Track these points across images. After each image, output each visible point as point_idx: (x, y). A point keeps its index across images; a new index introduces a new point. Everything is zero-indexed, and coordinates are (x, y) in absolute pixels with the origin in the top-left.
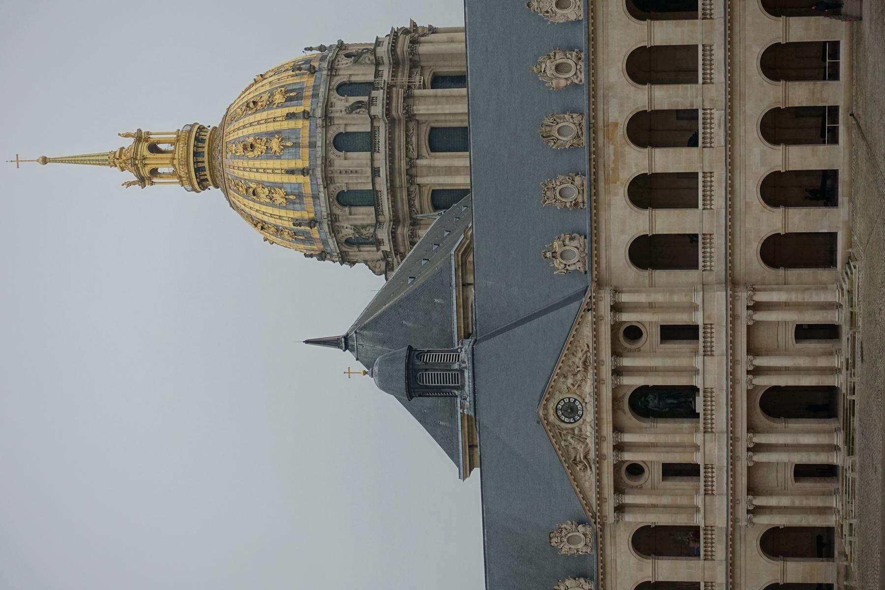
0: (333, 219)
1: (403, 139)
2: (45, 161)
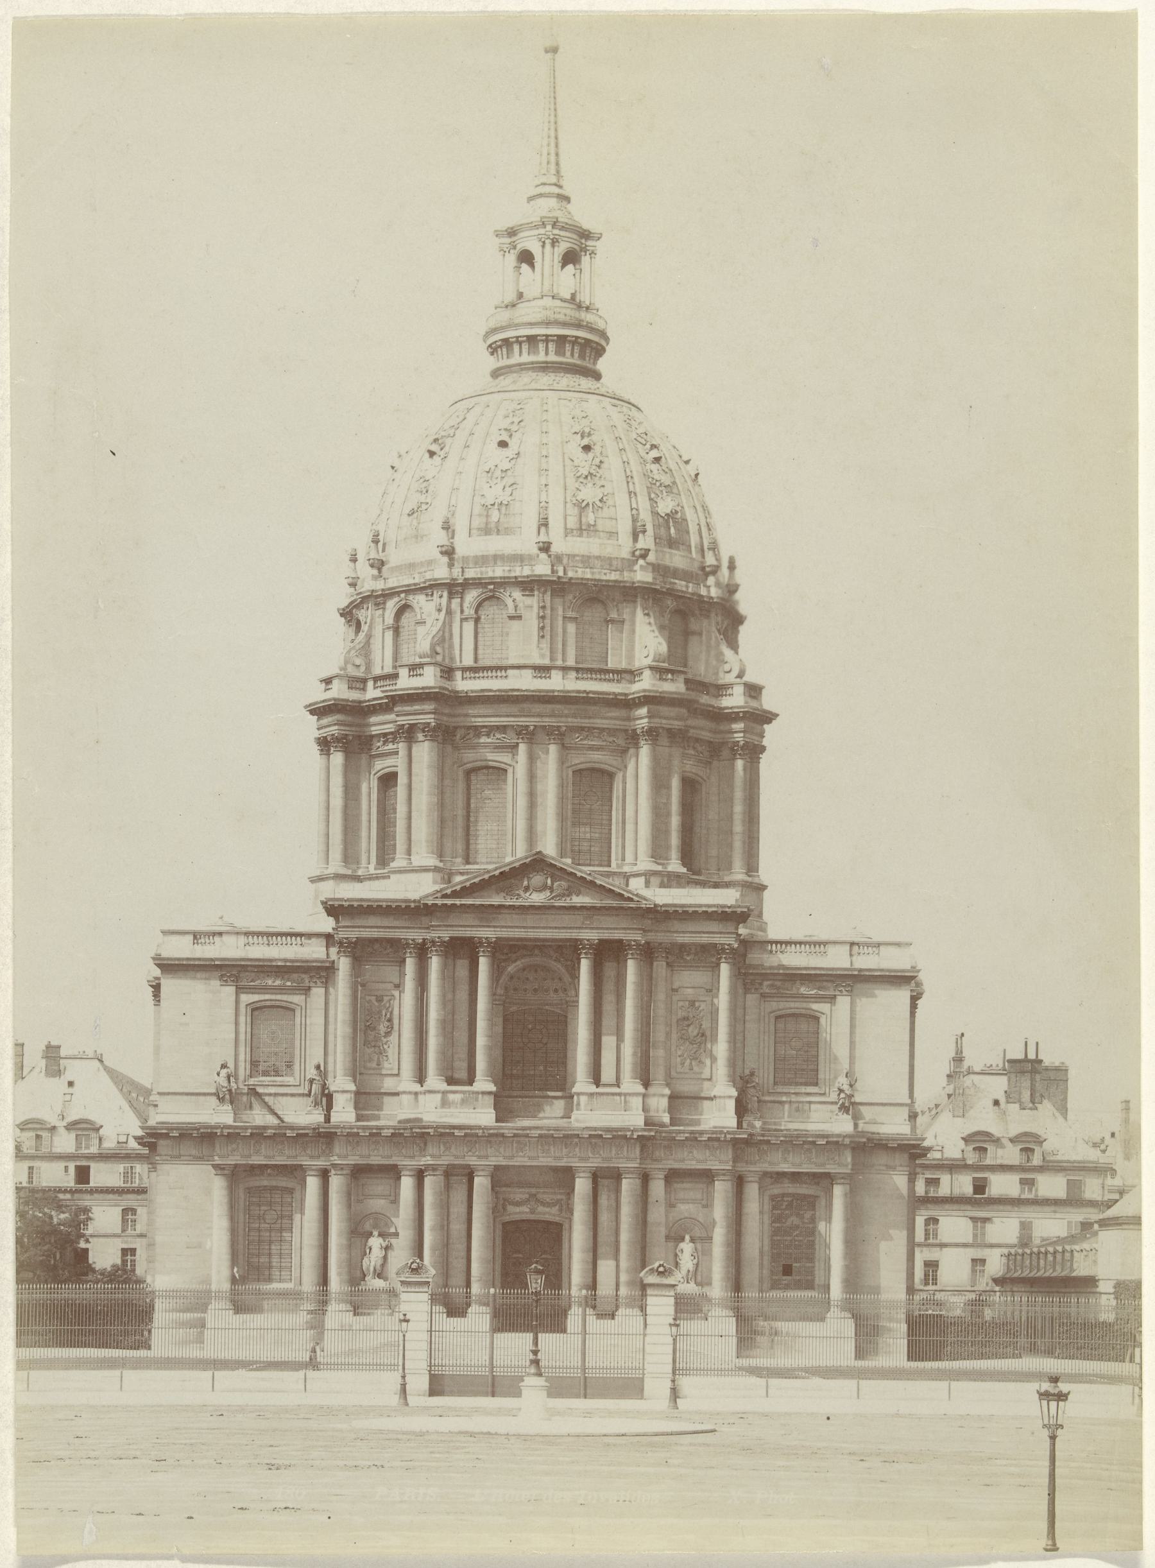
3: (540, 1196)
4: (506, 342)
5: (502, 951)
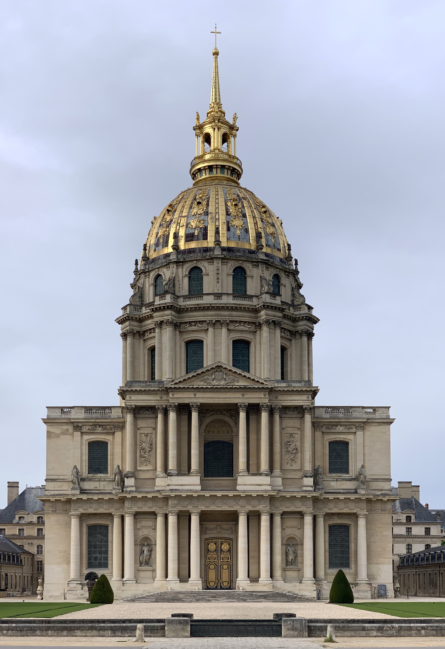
3: (222, 526)
4: (199, 170)
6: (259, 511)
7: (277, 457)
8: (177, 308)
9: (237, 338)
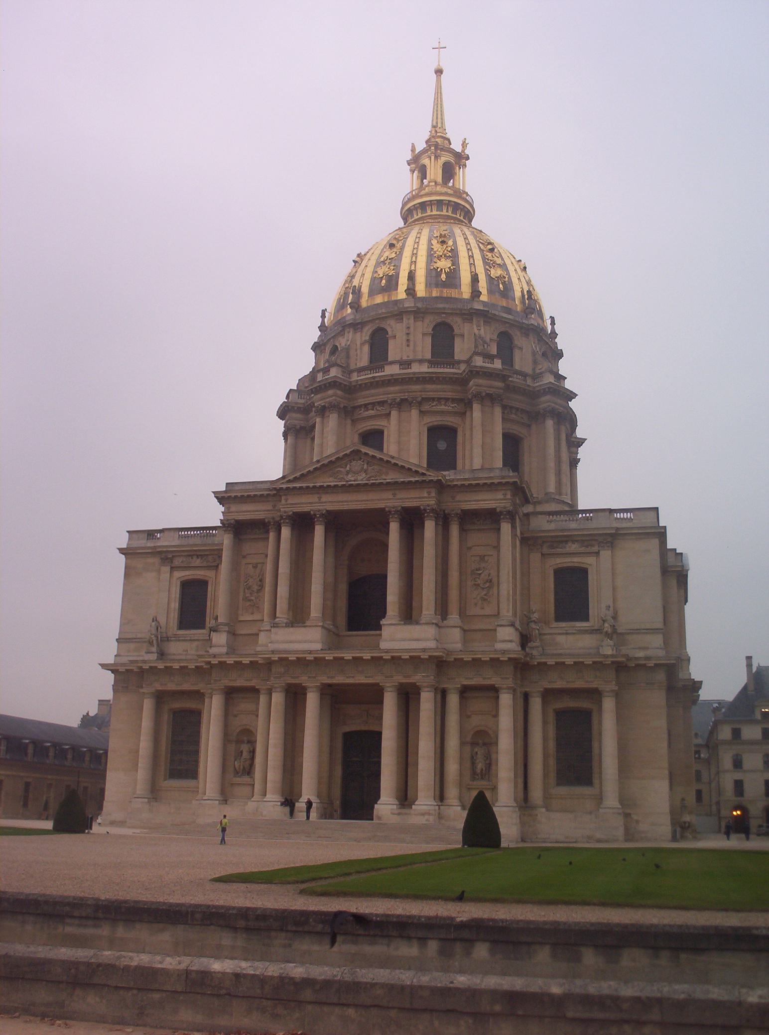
0: (356, 326)
1: (442, 395)
2: (439, 72)
4: (410, 211)
5: (337, 523)
6: (415, 683)
7: (454, 594)
8: (345, 385)
9: (435, 423)
